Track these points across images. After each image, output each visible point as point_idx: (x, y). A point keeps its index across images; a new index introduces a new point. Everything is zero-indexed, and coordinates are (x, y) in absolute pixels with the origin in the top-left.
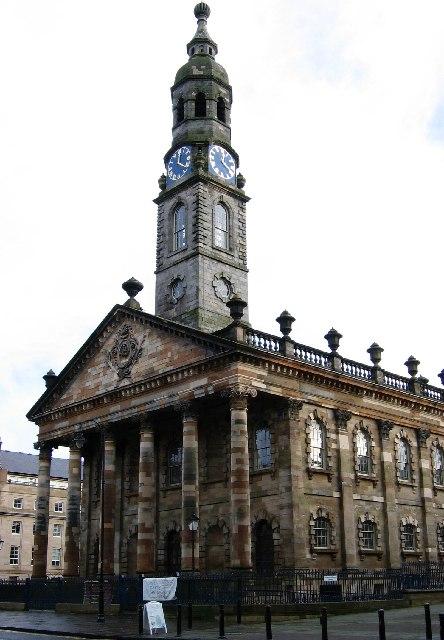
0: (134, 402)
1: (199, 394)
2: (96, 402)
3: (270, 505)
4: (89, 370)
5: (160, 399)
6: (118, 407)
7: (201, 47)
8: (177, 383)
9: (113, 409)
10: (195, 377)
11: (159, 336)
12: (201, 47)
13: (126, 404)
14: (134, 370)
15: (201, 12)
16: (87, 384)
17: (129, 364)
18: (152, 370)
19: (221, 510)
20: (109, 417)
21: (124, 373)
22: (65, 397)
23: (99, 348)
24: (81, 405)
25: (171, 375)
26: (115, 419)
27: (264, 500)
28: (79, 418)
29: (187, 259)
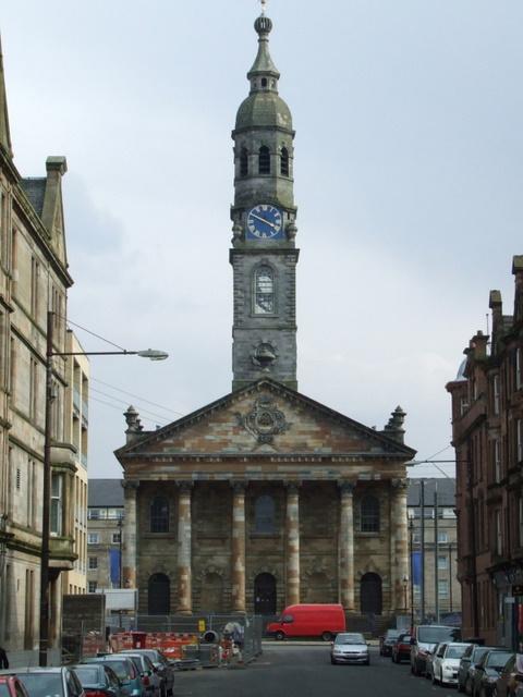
0: (281, 468)
1: (363, 477)
2: (228, 459)
3: (378, 562)
4: (210, 425)
5: (319, 473)
6: (259, 468)
7: (262, 78)
8: (339, 464)
9: (249, 468)
10: (358, 464)
11: (312, 417)
12: (262, 78)
13: (268, 468)
14: (278, 439)
15: (263, 27)
16: (208, 437)
17: (276, 432)
18: (305, 445)
19: (324, 561)
20: (246, 475)
21: (265, 439)
22: (170, 441)
23: (229, 407)
24: (208, 457)
25: (337, 458)
26: (255, 478)
27: (372, 557)
28: (198, 468)
29: (280, 328)
